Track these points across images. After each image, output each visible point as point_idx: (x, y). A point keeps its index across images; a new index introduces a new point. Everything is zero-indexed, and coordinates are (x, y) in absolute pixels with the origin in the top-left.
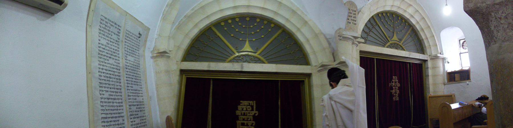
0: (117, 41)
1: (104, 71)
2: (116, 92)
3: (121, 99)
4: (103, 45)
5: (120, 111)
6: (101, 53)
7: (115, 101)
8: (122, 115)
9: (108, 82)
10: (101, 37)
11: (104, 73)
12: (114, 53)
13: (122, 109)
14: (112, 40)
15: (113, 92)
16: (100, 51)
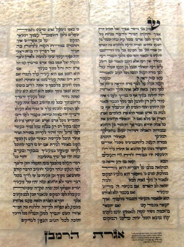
0: (70, 56)
1: (31, 117)
2: (61, 151)
3: (76, 163)
4: (26, 74)
5: (67, 185)
6: (22, 89)
7: (54, 166)
8: (75, 191)
9: (40, 135)
10: (24, 63)
11: (28, 121)
12: (63, 79)
13: (77, 182)
14: (56, 59)
15: (53, 151)
16: (20, 86)
